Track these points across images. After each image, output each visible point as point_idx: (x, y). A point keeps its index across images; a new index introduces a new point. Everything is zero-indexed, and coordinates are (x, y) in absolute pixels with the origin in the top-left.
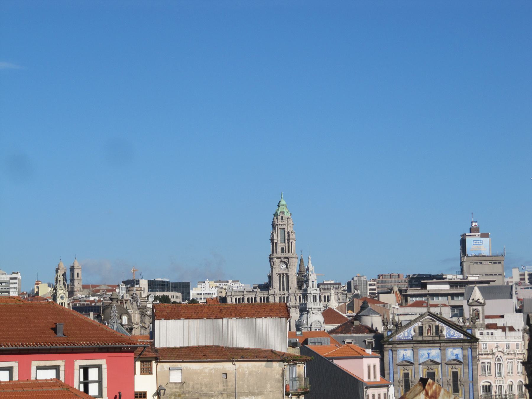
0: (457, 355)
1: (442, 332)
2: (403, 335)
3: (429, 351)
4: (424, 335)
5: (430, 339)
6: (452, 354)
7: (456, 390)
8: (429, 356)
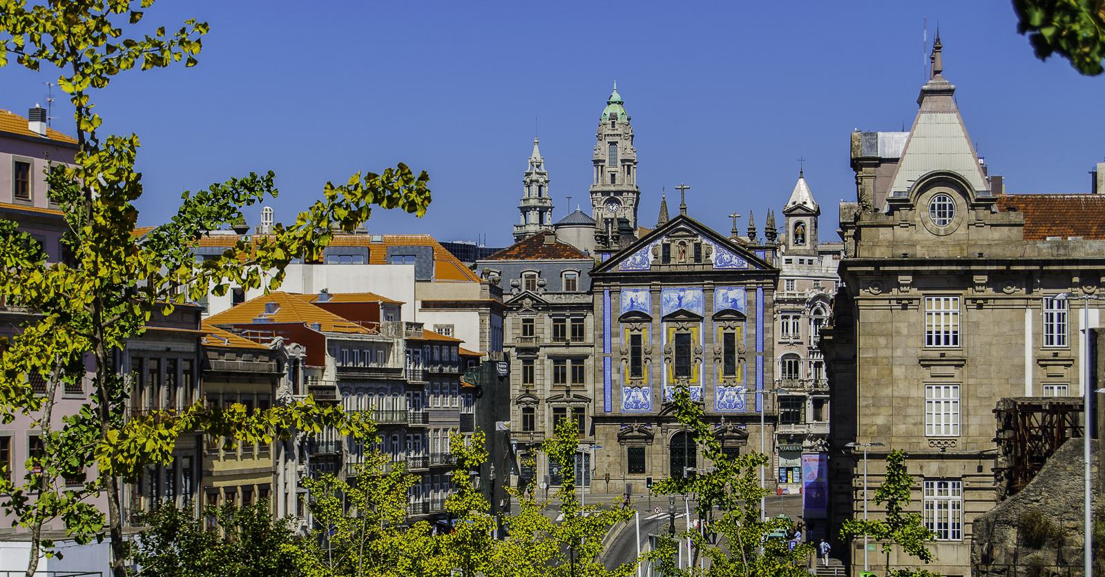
0: (734, 301)
1: (707, 256)
2: (633, 263)
3: (682, 294)
5: (685, 269)
7: (730, 370)
8: (680, 302)
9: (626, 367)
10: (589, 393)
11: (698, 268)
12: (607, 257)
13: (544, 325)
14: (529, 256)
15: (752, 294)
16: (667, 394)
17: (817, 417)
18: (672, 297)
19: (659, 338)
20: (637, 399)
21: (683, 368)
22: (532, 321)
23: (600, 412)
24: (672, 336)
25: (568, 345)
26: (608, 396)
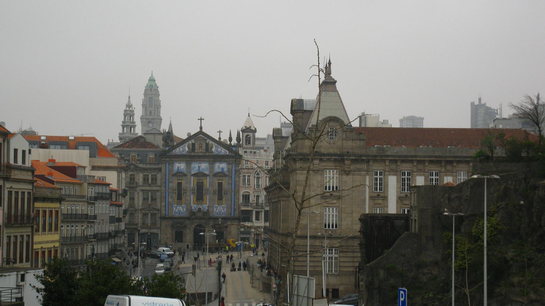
0: (223, 168)
1: (211, 148)
4: (196, 151)
6: (219, 168)
7: (220, 198)
9: (175, 196)
10: (159, 207)
11: (207, 154)
12: (167, 149)
13: (140, 178)
14: (133, 147)
15: (230, 166)
16: (193, 208)
17: (257, 219)
18: (196, 167)
19: (191, 183)
20: (179, 210)
21: (200, 198)
22: (134, 175)
23: (163, 215)
24: (195, 183)
25: (150, 185)
26: (167, 209)
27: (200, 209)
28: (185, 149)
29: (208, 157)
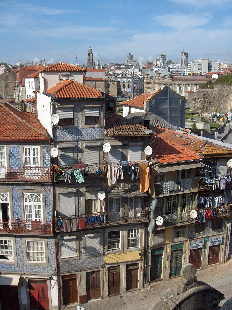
7: (129, 88)
17: (138, 93)
18: (123, 80)
27: (124, 91)
28: (120, 76)
29: (126, 78)
